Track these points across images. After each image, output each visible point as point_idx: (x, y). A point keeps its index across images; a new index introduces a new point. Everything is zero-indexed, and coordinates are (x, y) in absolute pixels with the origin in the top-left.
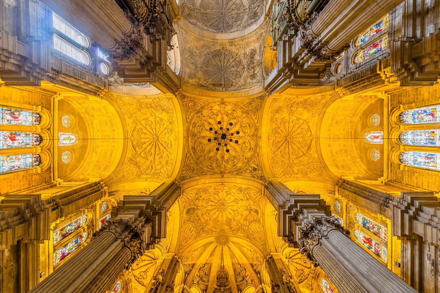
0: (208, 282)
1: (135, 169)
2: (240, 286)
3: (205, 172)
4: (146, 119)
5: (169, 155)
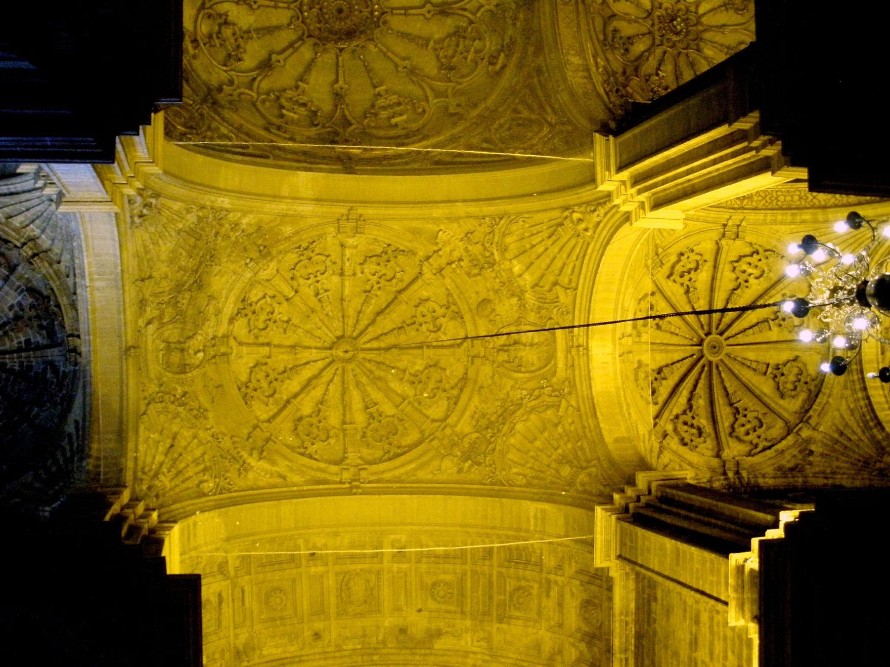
1: (519, 427)
3: (529, 76)
4: (247, 392)
5: (443, 261)
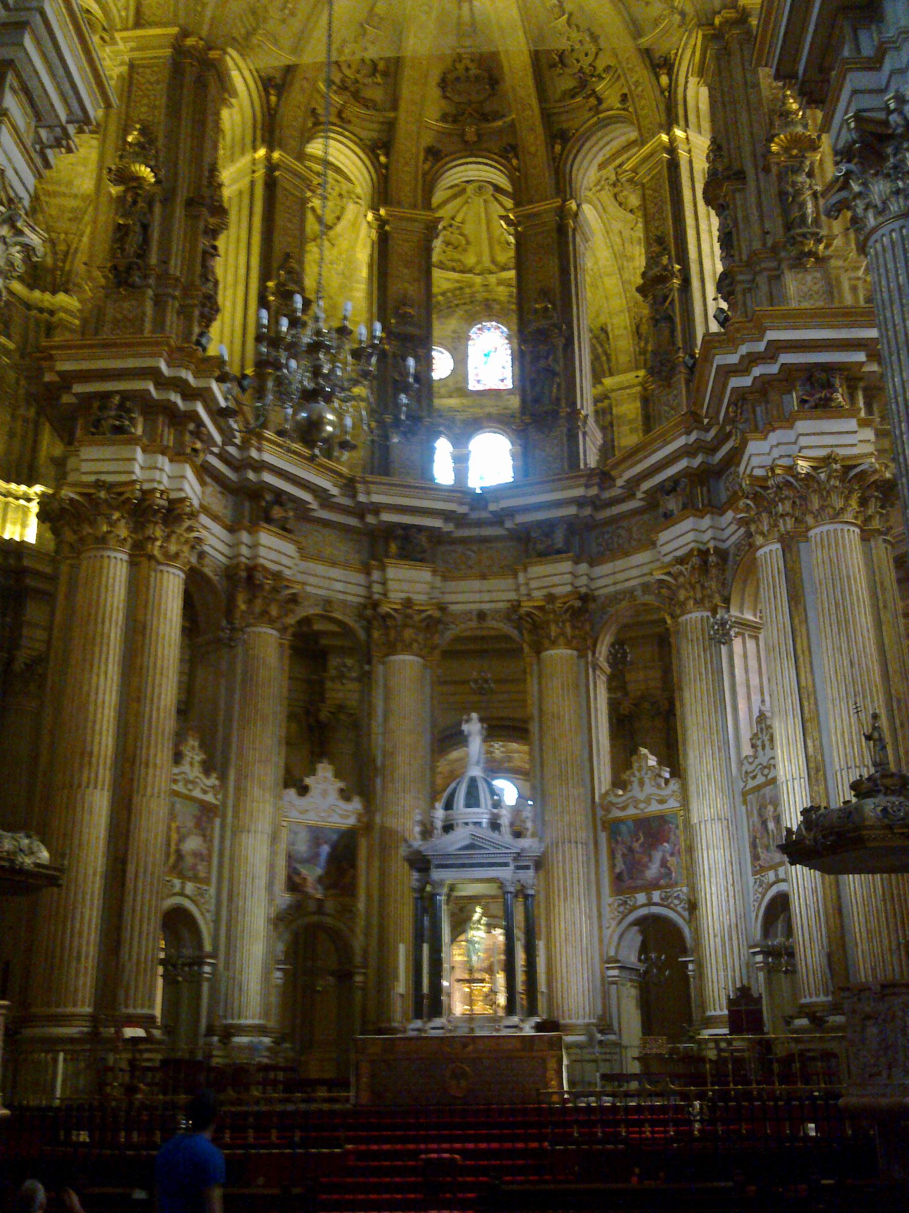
0: (395, 107)
2: (563, 117)
